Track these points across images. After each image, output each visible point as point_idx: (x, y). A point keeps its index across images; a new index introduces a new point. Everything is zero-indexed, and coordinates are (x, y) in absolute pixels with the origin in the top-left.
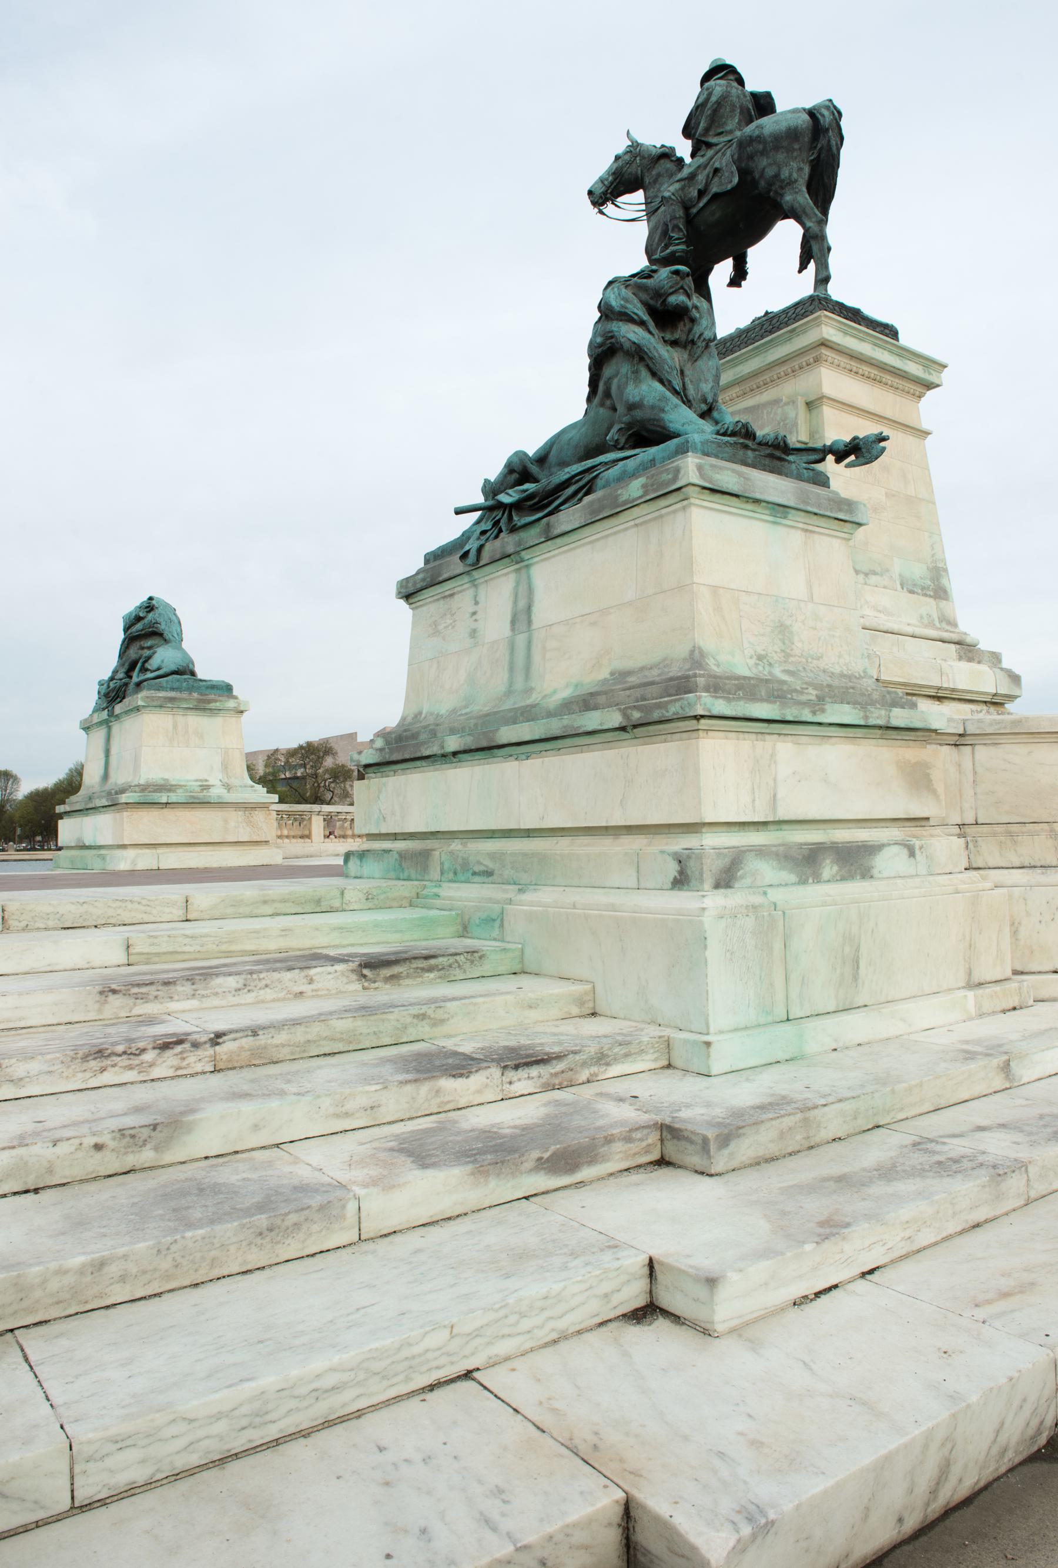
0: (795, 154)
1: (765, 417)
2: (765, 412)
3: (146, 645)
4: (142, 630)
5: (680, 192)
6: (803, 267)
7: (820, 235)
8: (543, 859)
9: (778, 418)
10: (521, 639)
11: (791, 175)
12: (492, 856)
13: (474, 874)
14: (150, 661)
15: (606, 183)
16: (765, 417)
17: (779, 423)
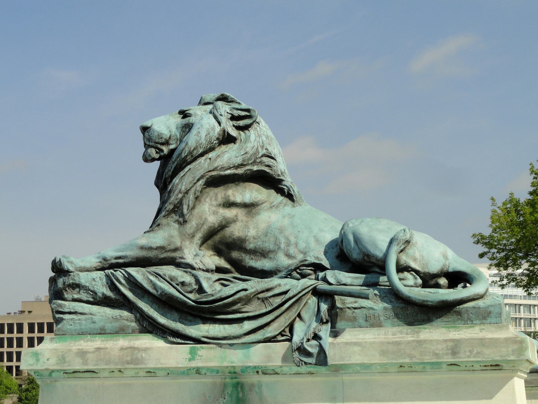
3: (238, 199)
4: (242, 165)
14: (410, 251)
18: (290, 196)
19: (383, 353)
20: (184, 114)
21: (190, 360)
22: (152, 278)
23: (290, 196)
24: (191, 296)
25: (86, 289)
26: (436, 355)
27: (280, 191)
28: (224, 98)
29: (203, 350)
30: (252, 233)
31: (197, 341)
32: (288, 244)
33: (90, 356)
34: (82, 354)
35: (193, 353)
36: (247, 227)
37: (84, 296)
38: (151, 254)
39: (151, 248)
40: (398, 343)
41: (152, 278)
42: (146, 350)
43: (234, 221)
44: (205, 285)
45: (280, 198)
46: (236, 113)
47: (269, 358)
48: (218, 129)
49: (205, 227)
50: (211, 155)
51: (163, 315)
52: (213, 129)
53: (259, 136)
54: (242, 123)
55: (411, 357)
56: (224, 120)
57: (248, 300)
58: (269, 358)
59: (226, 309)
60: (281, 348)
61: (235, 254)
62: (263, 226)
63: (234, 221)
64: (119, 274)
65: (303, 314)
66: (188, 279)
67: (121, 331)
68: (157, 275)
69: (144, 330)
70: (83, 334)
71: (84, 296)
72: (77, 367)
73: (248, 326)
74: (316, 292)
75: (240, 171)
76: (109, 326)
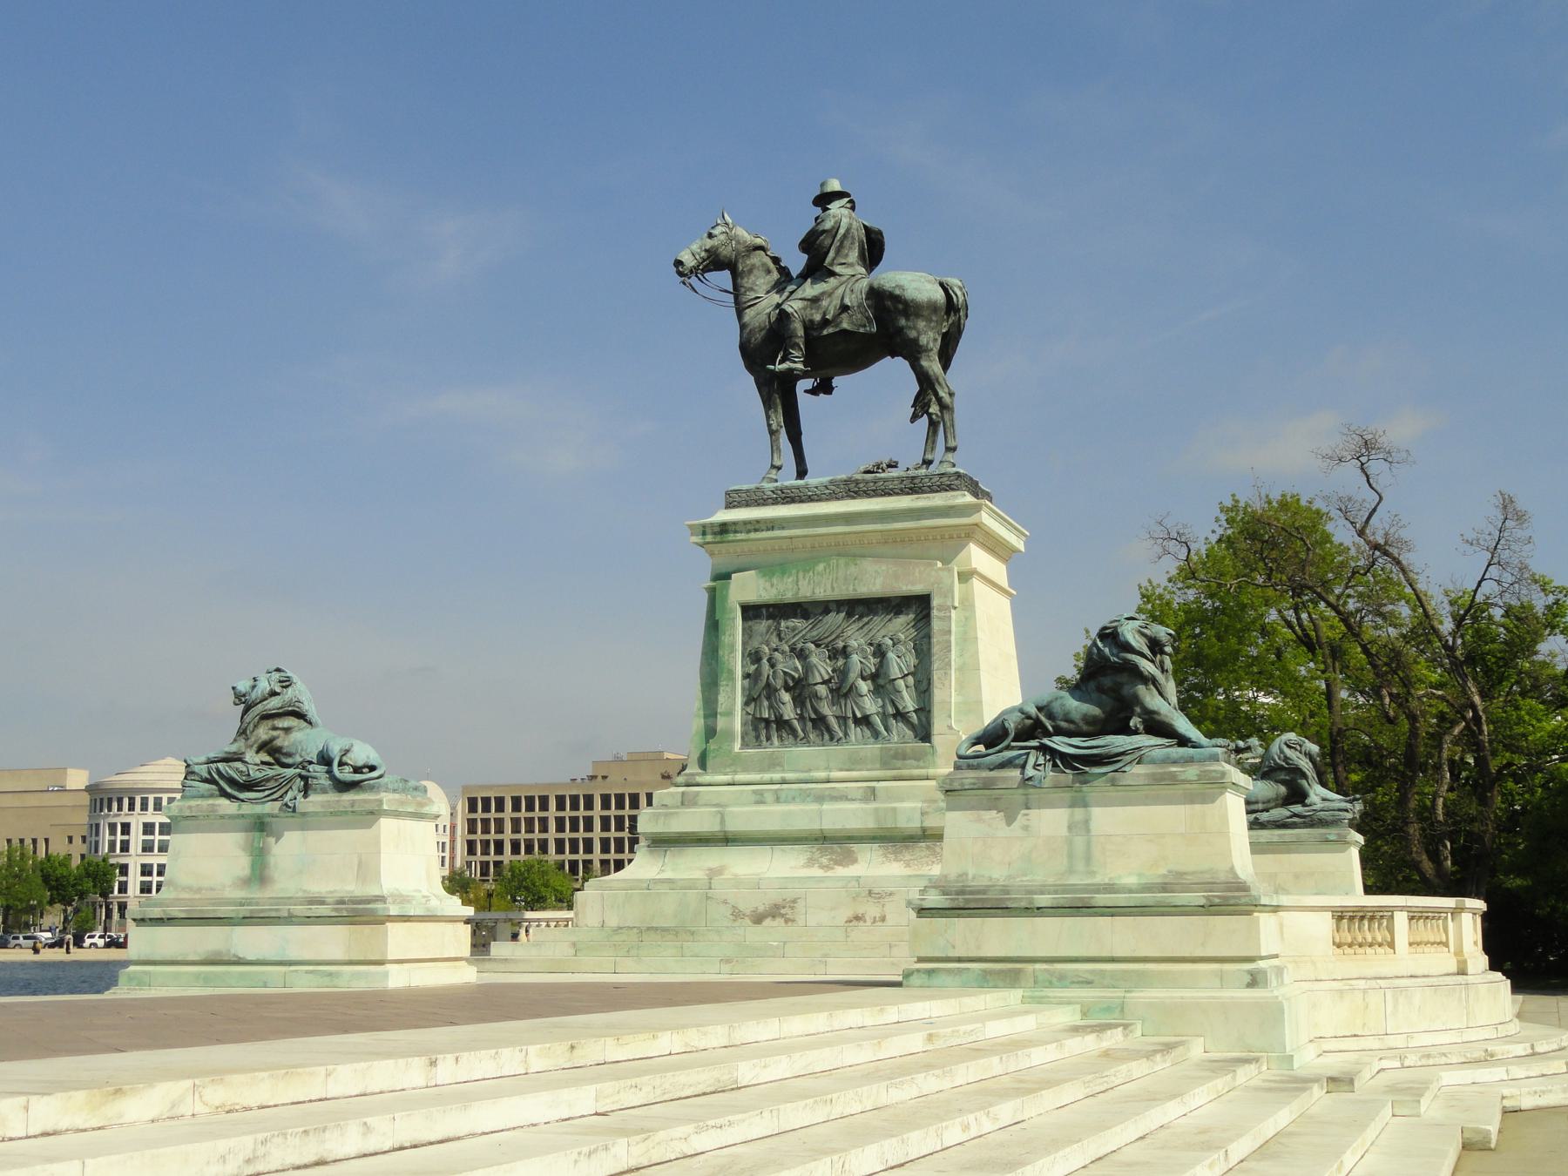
0: (932, 324)
1: (917, 574)
2: (917, 570)
3: (280, 726)
5: (803, 311)
6: (914, 418)
7: (951, 406)
8: (1141, 975)
9: (932, 580)
10: (1079, 841)
11: (928, 343)
12: (1092, 972)
13: (1073, 982)
14: (348, 755)
15: (698, 257)
16: (917, 574)
17: (933, 584)
18: (310, 723)
19: (323, 806)
20: (255, 680)
21: (239, 810)
22: (227, 768)
23: (310, 723)
24: (244, 778)
25: (198, 774)
26: (344, 807)
27: (306, 720)
28: (278, 670)
29: (244, 805)
30: (286, 744)
31: (243, 801)
32: (302, 750)
33: (193, 809)
34: (190, 807)
35: (239, 806)
36: (284, 741)
37: (197, 778)
38: (230, 756)
39: (230, 753)
40: (329, 801)
41: (227, 768)
42: (219, 805)
43: (278, 737)
44: (251, 772)
45: (306, 724)
46: (281, 679)
47: (272, 809)
48: (268, 689)
49: (260, 741)
50: (264, 703)
51: (230, 787)
52: (266, 689)
53: (294, 691)
54: (284, 684)
55: (334, 808)
56: (272, 683)
57: (268, 780)
58: (272, 809)
59: (257, 785)
60: (278, 804)
61: (277, 755)
62: (292, 740)
63: (278, 737)
64: (213, 766)
65: (293, 787)
66: (244, 769)
67: (211, 796)
68: (230, 767)
69: (221, 796)
70: (195, 797)
71: (197, 778)
72: (188, 814)
73: (267, 793)
74: (300, 776)
75: (280, 711)
76: (206, 794)
